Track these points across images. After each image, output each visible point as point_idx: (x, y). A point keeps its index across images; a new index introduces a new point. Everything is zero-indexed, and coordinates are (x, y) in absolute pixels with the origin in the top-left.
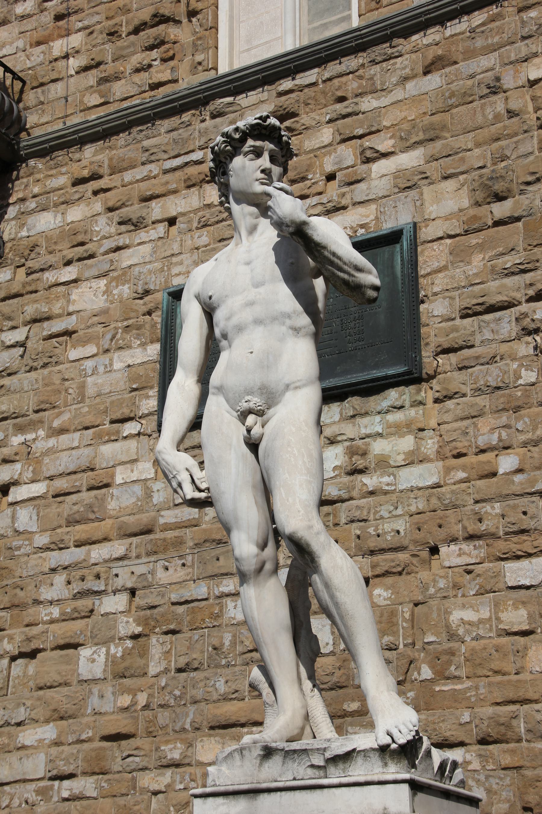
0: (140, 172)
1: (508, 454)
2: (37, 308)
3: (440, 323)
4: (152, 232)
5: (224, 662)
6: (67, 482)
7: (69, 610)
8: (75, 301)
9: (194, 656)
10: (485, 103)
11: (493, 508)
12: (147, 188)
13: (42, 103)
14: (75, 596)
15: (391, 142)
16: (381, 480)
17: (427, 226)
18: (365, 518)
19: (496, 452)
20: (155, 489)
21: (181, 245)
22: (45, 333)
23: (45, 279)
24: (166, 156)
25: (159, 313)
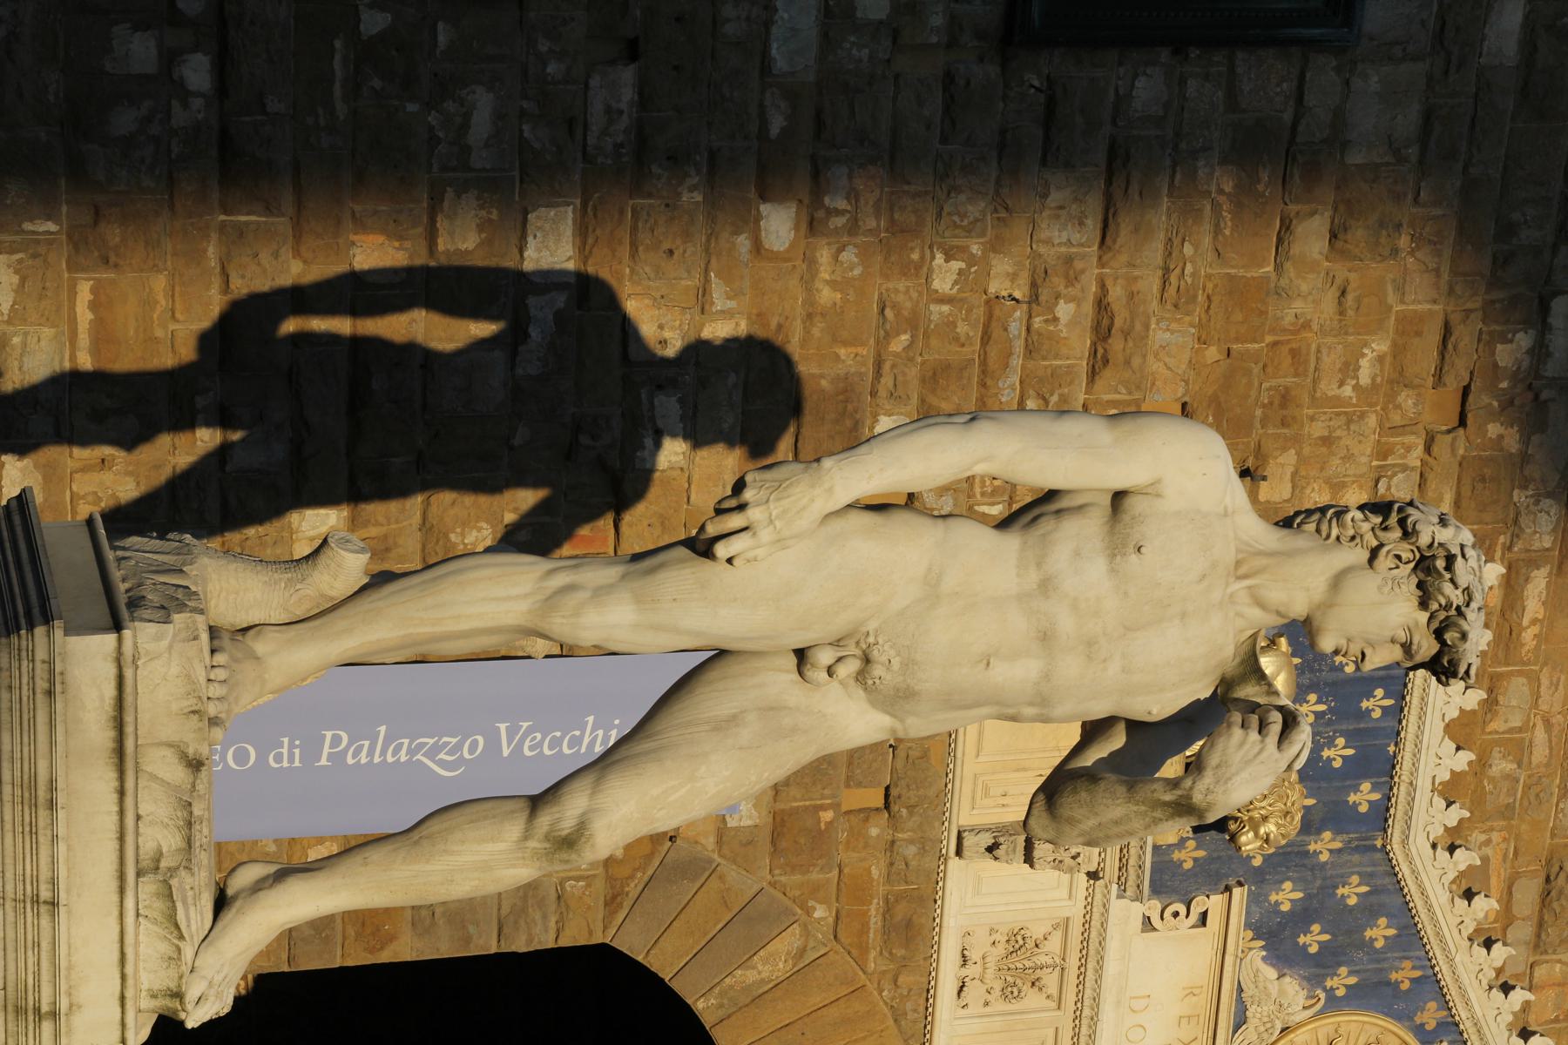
1: (797, 228)
3: (1117, 90)
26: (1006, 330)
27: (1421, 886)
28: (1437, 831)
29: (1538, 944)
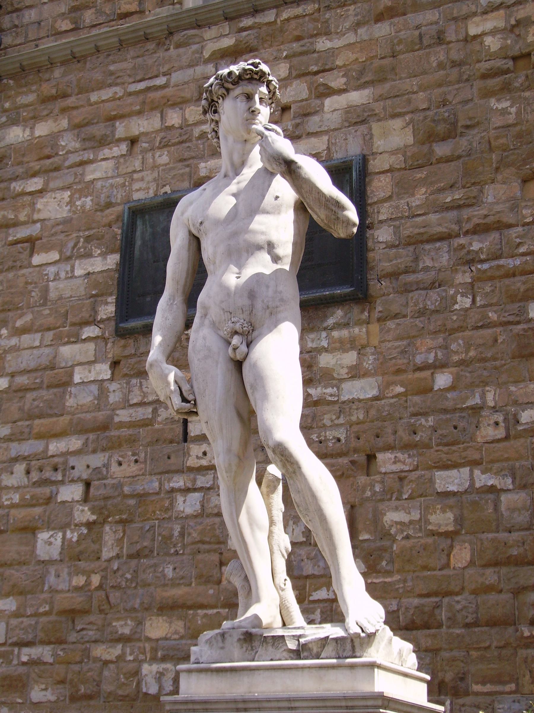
0: (106, 94)
2: (4, 216)
4: (115, 149)
5: (172, 551)
6: (28, 379)
7: (28, 497)
8: (39, 210)
9: (145, 544)
10: (430, 53)
11: (427, 421)
12: (110, 108)
13: (16, 26)
14: (34, 483)
15: (344, 80)
16: (325, 391)
17: (376, 159)
18: (309, 425)
19: (432, 371)
20: (111, 389)
21: (143, 163)
22: (10, 239)
23: (12, 188)
24: (131, 80)
25: (120, 224)
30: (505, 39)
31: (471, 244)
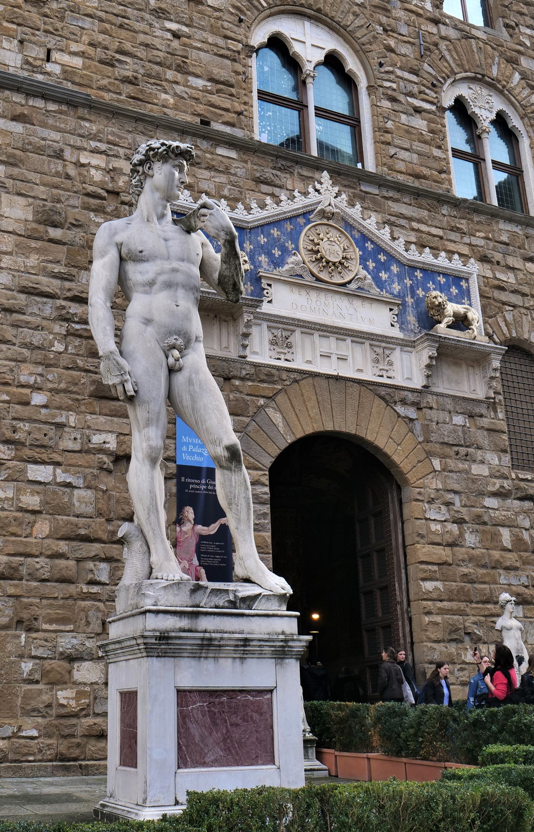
11: (24, 425)
26: (78, 330)
27: (261, 219)
28: (245, 212)
29: (281, 187)
30: (105, 176)
31: (70, 308)
